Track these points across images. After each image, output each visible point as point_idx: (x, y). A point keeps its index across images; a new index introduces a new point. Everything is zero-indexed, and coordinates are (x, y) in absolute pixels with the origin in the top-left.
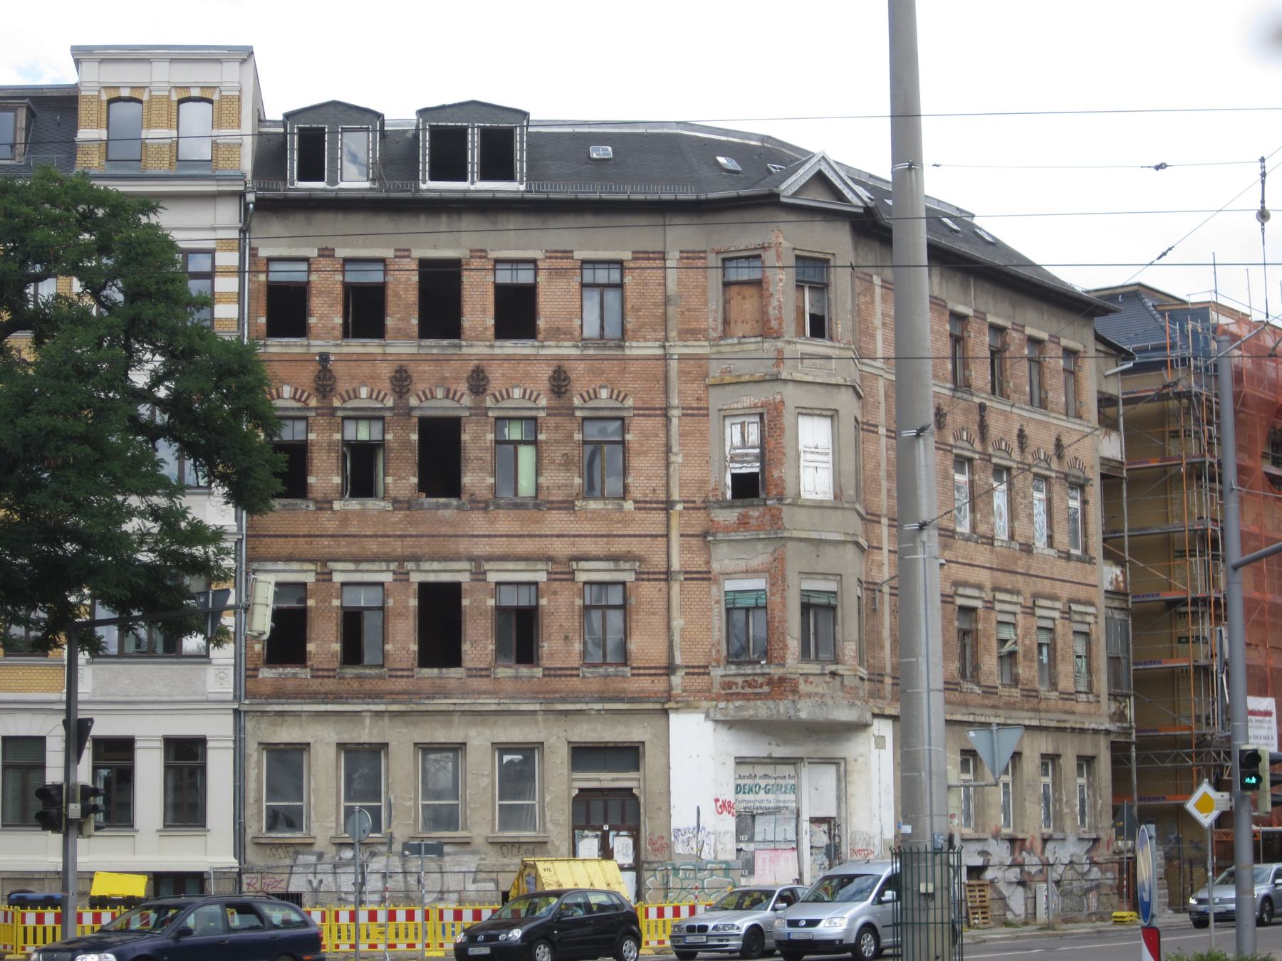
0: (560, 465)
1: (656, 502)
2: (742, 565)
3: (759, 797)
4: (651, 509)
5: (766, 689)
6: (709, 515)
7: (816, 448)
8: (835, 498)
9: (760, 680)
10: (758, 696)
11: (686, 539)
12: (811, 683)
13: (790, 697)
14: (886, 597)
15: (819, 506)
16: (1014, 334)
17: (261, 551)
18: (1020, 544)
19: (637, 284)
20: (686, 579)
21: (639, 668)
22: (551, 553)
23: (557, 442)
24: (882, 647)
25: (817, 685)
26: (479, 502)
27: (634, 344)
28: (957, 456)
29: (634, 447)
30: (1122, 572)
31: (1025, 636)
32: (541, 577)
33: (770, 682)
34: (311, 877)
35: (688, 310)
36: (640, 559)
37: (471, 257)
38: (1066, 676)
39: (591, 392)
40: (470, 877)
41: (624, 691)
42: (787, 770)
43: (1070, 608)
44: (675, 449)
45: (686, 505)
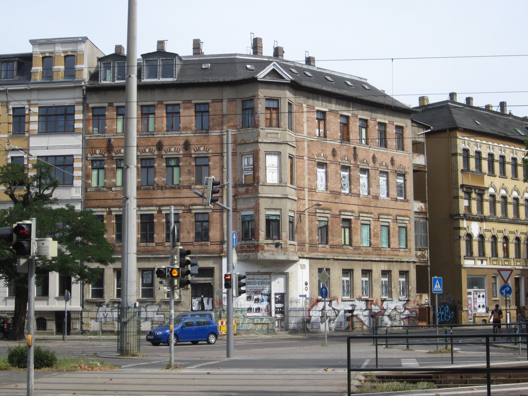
0: (187, 173)
2: (246, 206)
3: (255, 286)
5: (253, 249)
6: (236, 189)
9: (252, 246)
10: (251, 251)
12: (269, 247)
13: (261, 252)
14: (307, 216)
15: (273, 185)
16: (371, 122)
17: (89, 204)
18: (372, 196)
19: (213, 111)
21: (213, 242)
22: (184, 203)
23: (186, 166)
24: (304, 234)
25: (272, 247)
26: (160, 187)
27: (212, 131)
28: (342, 166)
29: (212, 167)
30: (424, 205)
31: (374, 229)
32: (181, 212)
33: (254, 247)
34: (104, 313)
35: (230, 119)
37: (158, 104)
38: (395, 242)
39: (197, 148)
40: (155, 313)
41: (208, 250)
42: (267, 277)
43: (396, 218)
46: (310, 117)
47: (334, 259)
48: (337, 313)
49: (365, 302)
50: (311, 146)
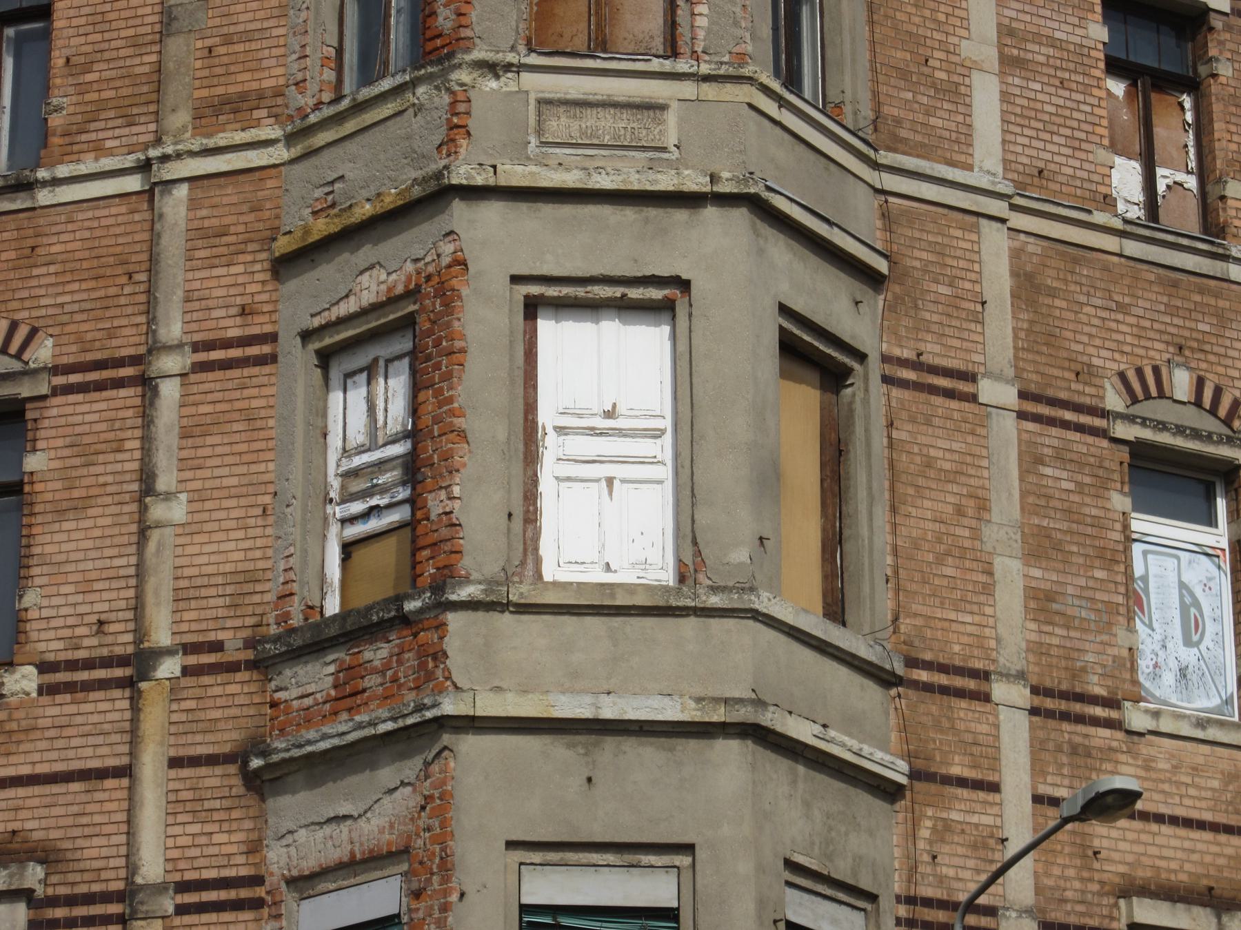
1: (107, 662)
4: (88, 686)
7: (609, 415)
8: (682, 579)
11: (186, 772)
20: (181, 910)
27: (63, 171)
29: (47, 492)
35: (228, 40)
36: (48, 856)
44: (164, 482)
45: (192, 660)
46: (1037, 38)
50: (1053, 293)
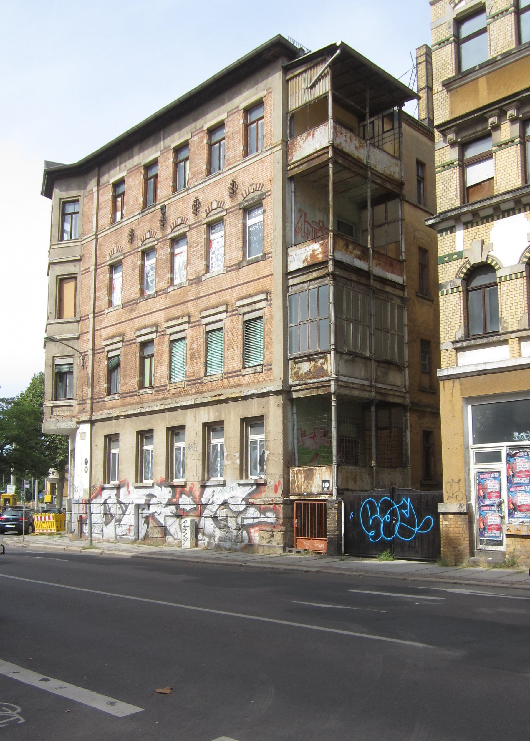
47: (126, 416)
48: (124, 509)
49: (170, 489)
